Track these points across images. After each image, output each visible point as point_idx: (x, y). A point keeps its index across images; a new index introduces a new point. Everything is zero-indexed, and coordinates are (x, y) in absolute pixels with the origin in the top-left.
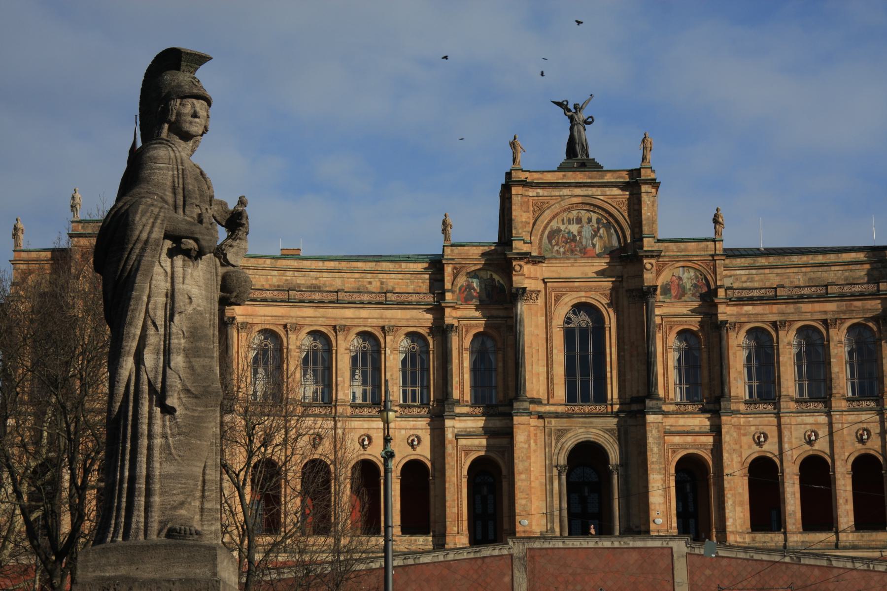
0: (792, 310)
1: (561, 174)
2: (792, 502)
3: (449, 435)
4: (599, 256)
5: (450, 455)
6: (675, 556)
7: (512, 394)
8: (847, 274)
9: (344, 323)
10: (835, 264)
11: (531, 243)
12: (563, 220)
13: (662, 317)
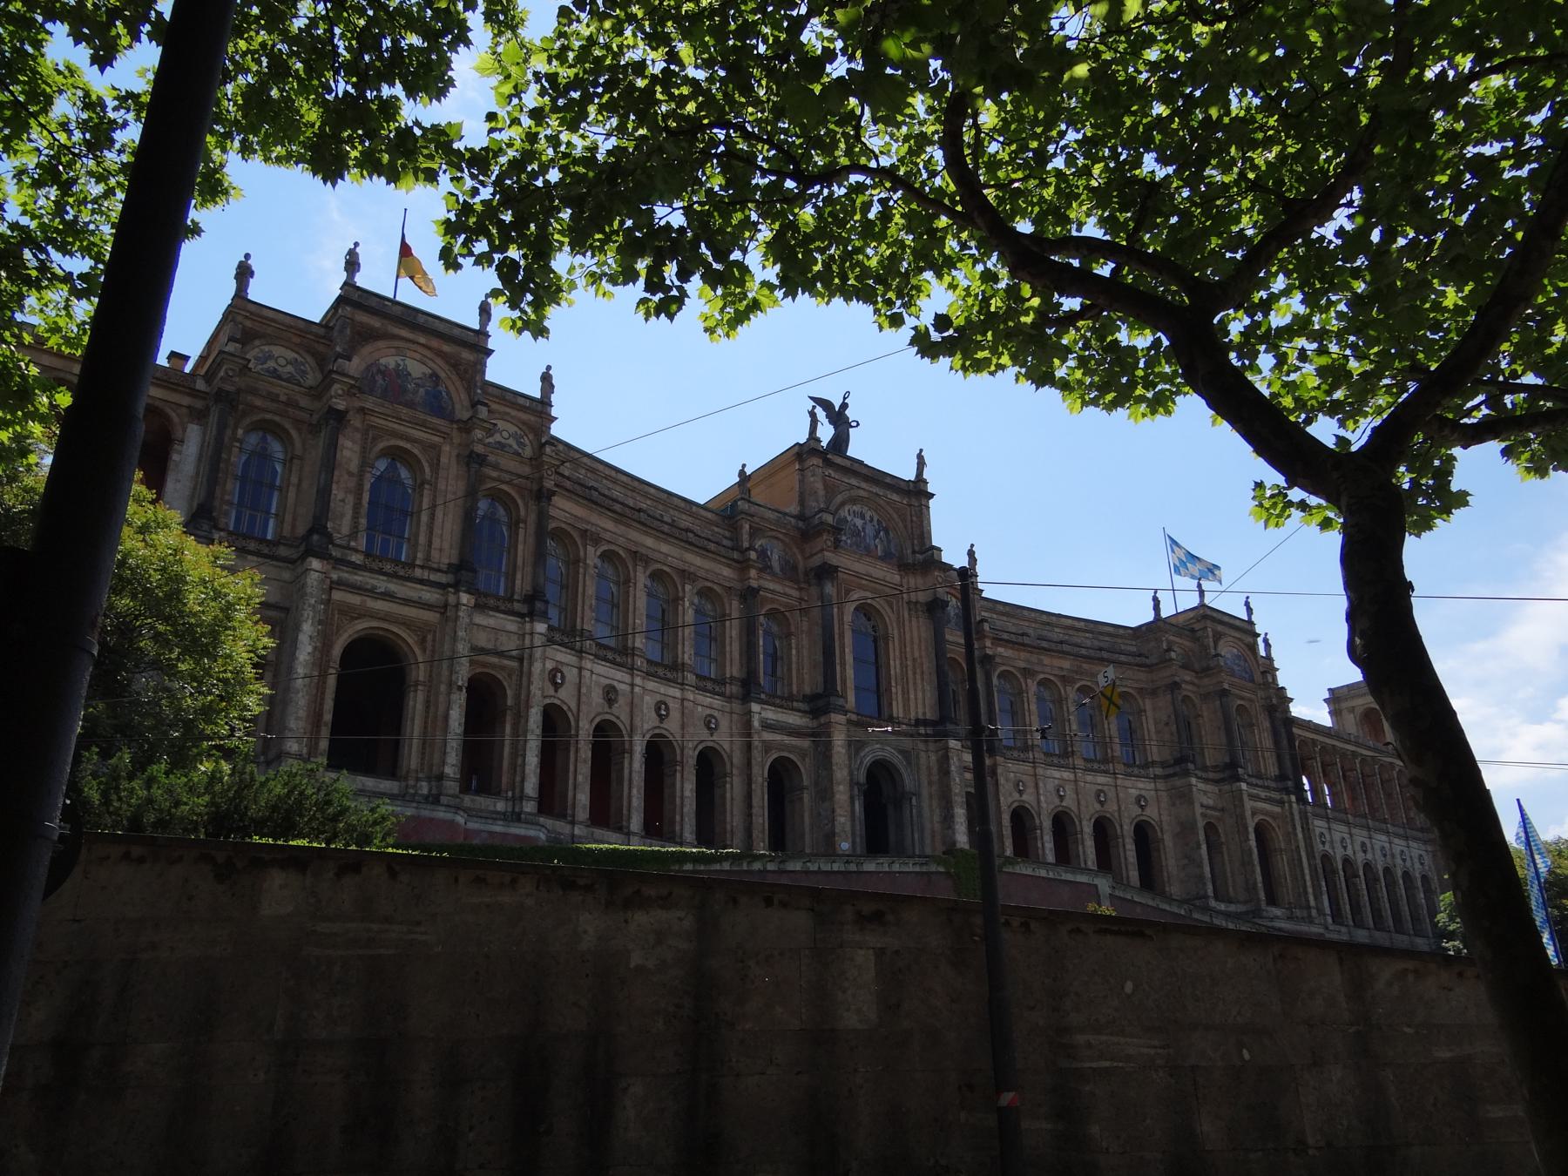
3: (756, 724)
4: (882, 559)
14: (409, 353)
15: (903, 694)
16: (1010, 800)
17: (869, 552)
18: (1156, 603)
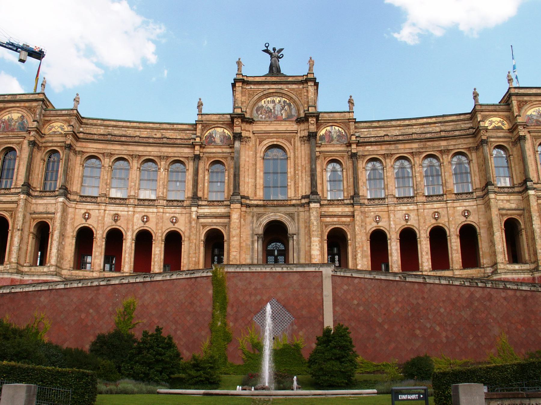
0: (394, 148)
2: (396, 255)
4: (285, 120)
5: (193, 227)
6: (324, 276)
8: (422, 130)
9: (137, 153)
10: (415, 125)
11: (246, 112)
12: (265, 102)
13: (320, 152)
14: (13, 111)
15: (295, 184)
18: (476, 96)
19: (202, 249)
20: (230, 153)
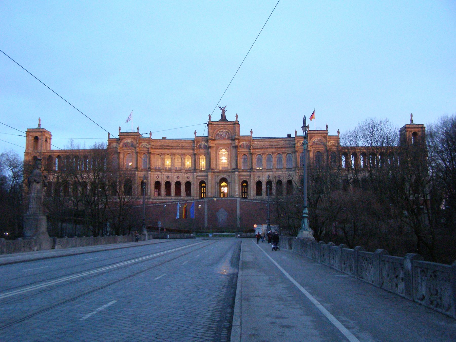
1: (219, 122)
7: (208, 168)
9: (174, 153)
10: (275, 141)
15: (230, 164)
16: (256, 180)
17: (224, 138)
19: (198, 188)
20: (207, 152)
